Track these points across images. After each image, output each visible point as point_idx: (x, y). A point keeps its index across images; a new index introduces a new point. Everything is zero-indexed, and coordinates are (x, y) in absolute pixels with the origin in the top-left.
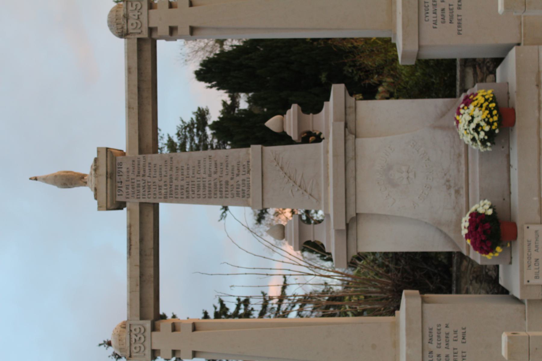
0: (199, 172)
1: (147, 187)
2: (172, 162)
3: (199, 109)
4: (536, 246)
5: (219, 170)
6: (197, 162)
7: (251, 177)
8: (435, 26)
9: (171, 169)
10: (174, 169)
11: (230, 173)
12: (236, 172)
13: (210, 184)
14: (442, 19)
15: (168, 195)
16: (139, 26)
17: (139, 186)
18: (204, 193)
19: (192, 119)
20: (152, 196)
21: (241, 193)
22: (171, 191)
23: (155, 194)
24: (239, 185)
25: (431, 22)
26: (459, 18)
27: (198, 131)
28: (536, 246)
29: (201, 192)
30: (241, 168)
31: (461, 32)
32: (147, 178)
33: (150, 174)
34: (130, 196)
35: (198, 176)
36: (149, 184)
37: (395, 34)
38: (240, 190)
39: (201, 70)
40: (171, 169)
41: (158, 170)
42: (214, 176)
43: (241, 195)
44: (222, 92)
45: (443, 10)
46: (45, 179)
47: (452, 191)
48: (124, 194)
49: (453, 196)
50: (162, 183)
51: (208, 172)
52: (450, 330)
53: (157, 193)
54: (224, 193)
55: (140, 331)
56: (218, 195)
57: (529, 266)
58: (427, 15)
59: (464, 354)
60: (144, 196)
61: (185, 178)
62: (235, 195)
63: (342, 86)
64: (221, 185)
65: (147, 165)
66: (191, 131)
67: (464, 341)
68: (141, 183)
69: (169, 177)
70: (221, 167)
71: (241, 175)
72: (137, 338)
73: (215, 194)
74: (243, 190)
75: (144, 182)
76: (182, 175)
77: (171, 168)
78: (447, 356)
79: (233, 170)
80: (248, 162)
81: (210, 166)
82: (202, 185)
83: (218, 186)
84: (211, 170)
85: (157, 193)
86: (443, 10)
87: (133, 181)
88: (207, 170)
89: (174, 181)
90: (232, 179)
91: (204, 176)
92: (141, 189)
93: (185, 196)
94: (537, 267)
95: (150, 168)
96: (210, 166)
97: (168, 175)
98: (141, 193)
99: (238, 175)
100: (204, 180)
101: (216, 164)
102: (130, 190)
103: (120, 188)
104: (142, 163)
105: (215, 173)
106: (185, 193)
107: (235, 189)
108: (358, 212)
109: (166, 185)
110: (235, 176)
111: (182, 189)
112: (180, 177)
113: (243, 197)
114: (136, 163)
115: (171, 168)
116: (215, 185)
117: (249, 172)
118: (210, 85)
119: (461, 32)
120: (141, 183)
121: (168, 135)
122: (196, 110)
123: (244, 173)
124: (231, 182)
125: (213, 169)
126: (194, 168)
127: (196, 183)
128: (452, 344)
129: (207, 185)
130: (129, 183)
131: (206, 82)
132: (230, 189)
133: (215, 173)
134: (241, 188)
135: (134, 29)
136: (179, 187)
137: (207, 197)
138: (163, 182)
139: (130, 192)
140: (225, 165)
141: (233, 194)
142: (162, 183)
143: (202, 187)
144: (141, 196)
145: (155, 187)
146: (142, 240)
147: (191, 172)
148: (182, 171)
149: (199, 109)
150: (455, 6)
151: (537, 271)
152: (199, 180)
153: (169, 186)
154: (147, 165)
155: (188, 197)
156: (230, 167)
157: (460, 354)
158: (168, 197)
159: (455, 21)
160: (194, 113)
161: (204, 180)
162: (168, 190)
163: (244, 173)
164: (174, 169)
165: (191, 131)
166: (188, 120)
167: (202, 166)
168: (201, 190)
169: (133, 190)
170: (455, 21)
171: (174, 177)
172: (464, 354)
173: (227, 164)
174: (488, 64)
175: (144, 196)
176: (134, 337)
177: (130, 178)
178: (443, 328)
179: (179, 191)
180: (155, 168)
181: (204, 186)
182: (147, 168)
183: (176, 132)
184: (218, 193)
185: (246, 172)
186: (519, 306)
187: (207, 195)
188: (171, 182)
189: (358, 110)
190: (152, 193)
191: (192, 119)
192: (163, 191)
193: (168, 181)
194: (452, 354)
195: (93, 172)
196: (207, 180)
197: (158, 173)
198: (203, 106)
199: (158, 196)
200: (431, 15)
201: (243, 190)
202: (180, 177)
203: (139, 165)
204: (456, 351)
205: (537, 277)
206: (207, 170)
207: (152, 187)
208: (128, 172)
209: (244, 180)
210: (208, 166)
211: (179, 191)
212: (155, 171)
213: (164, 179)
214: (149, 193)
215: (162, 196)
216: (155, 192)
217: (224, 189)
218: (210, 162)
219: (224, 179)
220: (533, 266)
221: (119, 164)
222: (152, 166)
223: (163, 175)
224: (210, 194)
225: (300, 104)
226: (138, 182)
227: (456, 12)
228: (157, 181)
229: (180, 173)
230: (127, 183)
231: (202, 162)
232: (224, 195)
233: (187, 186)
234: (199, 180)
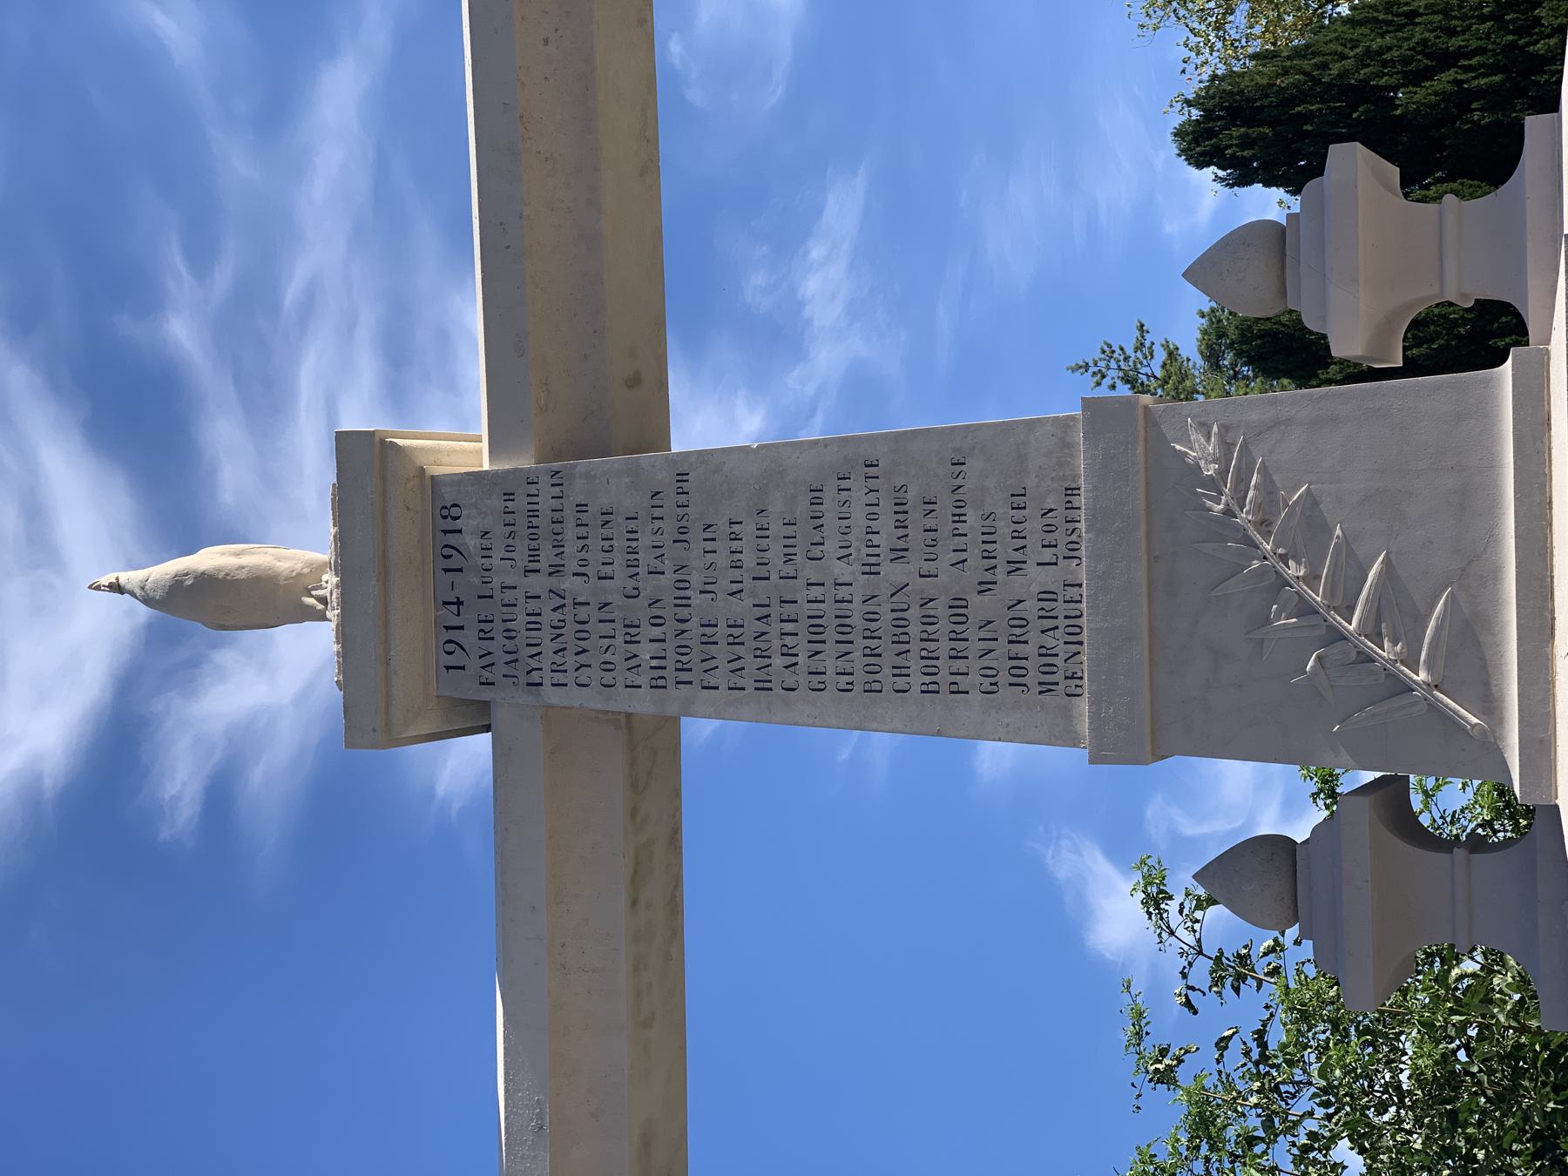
0: (816, 551)
1: (570, 629)
2: (683, 499)
5: (915, 535)
10: (696, 534)
13: (871, 617)
15: (669, 673)
18: (842, 664)
20: (593, 675)
22: (683, 650)
23: (607, 667)
24: (1022, 622)
29: (830, 664)
30: (1033, 527)
32: (569, 584)
33: (584, 563)
34: (495, 675)
35: (810, 572)
36: (583, 613)
38: (1030, 649)
42: (893, 573)
43: (1033, 678)
48: (474, 664)
51: (860, 551)
56: (917, 680)
60: (559, 677)
61: (748, 584)
62: (1004, 678)
64: (928, 620)
65: (569, 514)
69: (668, 579)
70: (930, 523)
71: (1032, 570)
73: (900, 671)
74: (1044, 652)
75: (558, 602)
77: (683, 531)
79: (989, 536)
81: (873, 517)
82: (830, 622)
84: (875, 539)
87: (509, 596)
89: (697, 599)
90: (985, 587)
91: (842, 571)
92: (546, 634)
95: (582, 531)
96: (873, 517)
100: (843, 592)
103: (453, 635)
106: (751, 663)
107: (1002, 646)
110: (1000, 574)
112: (724, 584)
113: (1047, 688)
115: (683, 531)
116: (900, 623)
123: (1047, 555)
124: (980, 606)
125: (886, 537)
126: (790, 530)
129: (857, 621)
132: (975, 647)
133: (899, 554)
134: (1034, 638)
136: (722, 630)
137: (858, 688)
138: (642, 601)
139: (500, 657)
140: (945, 507)
141: (989, 673)
143: (831, 635)
145: (606, 629)
147: (775, 554)
148: (735, 545)
152: (816, 592)
153: (671, 626)
154: (569, 514)
155: (763, 687)
158: (670, 683)
161: (843, 592)
162: (670, 645)
163: (1047, 555)
167: (830, 521)
168: (831, 649)
169: (509, 645)
171: (696, 579)
173: (959, 504)
175: (559, 677)
177: (496, 583)
179: (721, 653)
180: (607, 532)
181: (844, 628)
182: (570, 532)
184: (915, 665)
185: (1062, 550)
187: (859, 678)
192: (646, 651)
193: (669, 600)
197: (619, 558)
199: (621, 676)
201: (1044, 652)
202: (724, 584)
209: (1047, 596)
210: (859, 519)
212: (606, 544)
214: (582, 659)
216: (608, 657)
218: (872, 498)
221: (445, 512)
223: (642, 570)
226: (533, 605)
228: (617, 600)
229: (722, 559)
231: (830, 497)
232: (944, 678)
233: (760, 626)
234: (816, 592)
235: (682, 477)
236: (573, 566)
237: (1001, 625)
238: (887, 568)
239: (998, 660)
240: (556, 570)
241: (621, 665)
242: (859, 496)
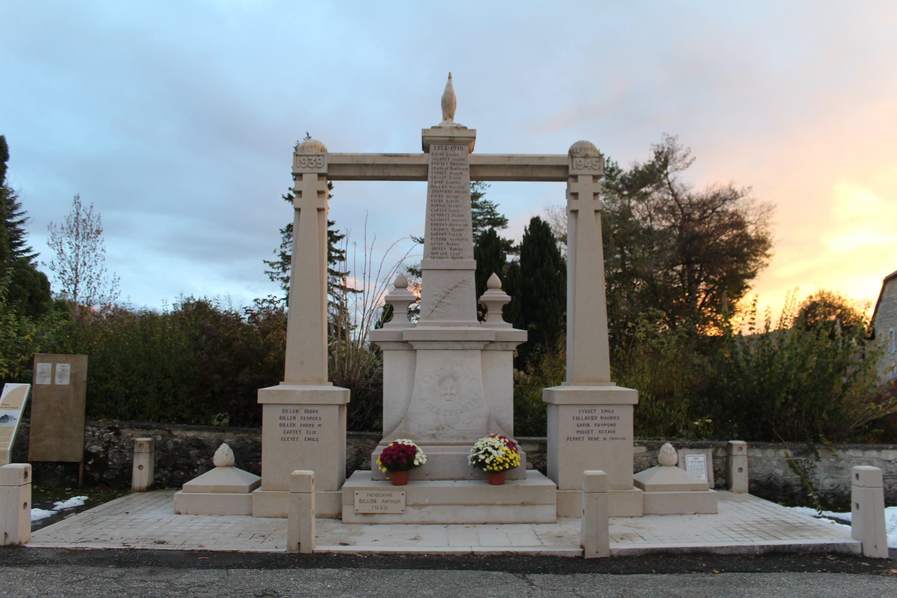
1: (442, 171)
3: (507, 220)
4: (387, 501)
5: (456, 233)
6: (462, 214)
7: (449, 260)
8: (575, 418)
9: (456, 192)
10: (456, 194)
11: (452, 242)
12: (453, 247)
13: (443, 225)
15: (434, 189)
16: (579, 167)
17: (443, 164)
19: (499, 214)
20: (434, 175)
21: (436, 251)
22: (438, 191)
23: (435, 177)
24: (442, 249)
25: (578, 415)
26: (581, 439)
27: (488, 219)
28: (387, 501)
30: (456, 252)
32: (449, 171)
34: (434, 156)
35: (450, 215)
36: (444, 173)
37: (569, 385)
38: (438, 251)
39: (540, 222)
40: (456, 192)
41: (456, 181)
43: (434, 251)
44: (521, 239)
45: (588, 425)
46: (449, 85)
47: (434, 432)
49: (430, 432)
50: (444, 183)
51: (453, 223)
52: (316, 428)
53: (437, 179)
54: (436, 237)
55: (318, 164)
56: (433, 232)
57: (370, 495)
59: (295, 439)
63: (526, 340)
64: (443, 234)
65: (460, 171)
66: (488, 213)
67: (307, 439)
68: (445, 166)
69: (450, 189)
72: (312, 161)
73: (435, 229)
74: (438, 253)
76: (452, 201)
78: (294, 425)
79: (456, 244)
80: (462, 258)
81: (459, 225)
82: (442, 217)
83: (441, 232)
85: (437, 179)
86: (588, 425)
88: (455, 222)
89: (446, 194)
90: (448, 244)
91: (450, 219)
93: (433, 203)
94: (369, 501)
96: (459, 225)
97: (452, 189)
98: (436, 166)
99: (451, 249)
101: (460, 230)
102: (439, 157)
104: (462, 167)
105: (453, 230)
106: (436, 203)
107: (439, 246)
108: (418, 351)
109: (443, 187)
110: (450, 246)
111: (439, 201)
112: (449, 199)
113: (432, 253)
114: (462, 162)
116: (443, 229)
117: (453, 258)
118: (527, 229)
120: (445, 166)
121: (485, 194)
122: (506, 217)
124: (444, 243)
125: (456, 228)
127: (444, 213)
128: (304, 429)
129: (442, 222)
130: (445, 156)
131: (530, 226)
132: (438, 241)
133: (453, 230)
134: (440, 251)
135: (576, 163)
136: (441, 198)
139: (437, 157)
140: (460, 237)
141: (434, 244)
142: (444, 183)
143: (440, 218)
144: (434, 166)
146: (396, 166)
147: (453, 208)
149: (507, 220)
150: (591, 435)
151: (366, 501)
153: (442, 190)
154: (460, 171)
155: (432, 205)
156: (457, 242)
157: (295, 435)
159: (579, 435)
160: (503, 216)
162: (438, 189)
164: (456, 194)
165: (488, 213)
166: (497, 210)
167: (458, 218)
168: (438, 217)
170: (579, 435)
171: (449, 194)
172: (295, 439)
174: (541, 463)
176: (313, 158)
178: (318, 422)
179: (438, 198)
181: (442, 220)
182: (458, 171)
183: (487, 200)
184: (436, 232)
186: (336, 486)
187: (433, 222)
188: (446, 192)
189: (505, 352)
190: (436, 175)
191: (499, 214)
192: (438, 185)
193: (447, 189)
194: (296, 430)
195: (455, 126)
196: (447, 222)
197: (453, 180)
198: (509, 224)
200: (584, 415)
201: (438, 253)
202: (449, 199)
203: (461, 164)
204: (298, 432)
205: (360, 501)
206: (455, 222)
207: (441, 176)
208: (455, 155)
209: (446, 254)
211: (438, 198)
213: (448, 185)
215: (433, 184)
217: (438, 237)
219: (447, 237)
220: (370, 498)
222: (460, 176)
224: (435, 224)
225: (510, 303)
227: (586, 436)
228: (446, 179)
229: (453, 199)
230: (445, 155)
231: (463, 218)
232: (434, 236)
235: (466, 192)
236: (452, 171)
237: (442, 246)
238: (451, 227)
239: (436, 246)
240: (451, 168)
241: (435, 180)
242: (462, 223)
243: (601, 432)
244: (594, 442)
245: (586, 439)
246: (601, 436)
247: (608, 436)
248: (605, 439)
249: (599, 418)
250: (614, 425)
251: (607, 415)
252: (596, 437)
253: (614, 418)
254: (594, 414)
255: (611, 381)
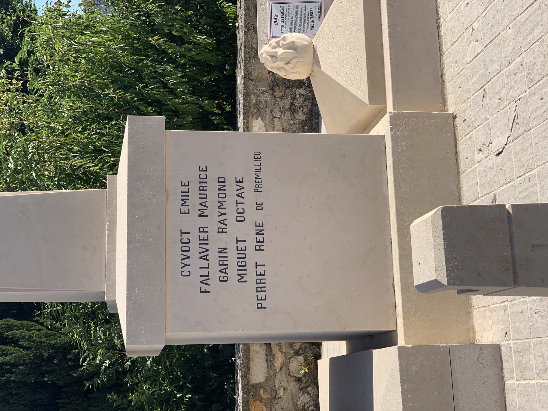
14: (220, 271)
25: (195, 279)
26: (260, 270)
31: (264, 303)
58: (186, 262)
86: (223, 251)
119: (264, 303)
150: (251, 244)
159: (251, 277)
170: (251, 277)
200: (195, 262)
227: (253, 257)
243: (241, 218)
244: (267, 235)
245: (259, 257)
246: (252, 215)
247: (250, 197)
248: (259, 207)
249: (203, 222)
250: (221, 181)
251: (194, 199)
252: (254, 230)
253: (203, 181)
254: (194, 237)
255: (104, 186)
